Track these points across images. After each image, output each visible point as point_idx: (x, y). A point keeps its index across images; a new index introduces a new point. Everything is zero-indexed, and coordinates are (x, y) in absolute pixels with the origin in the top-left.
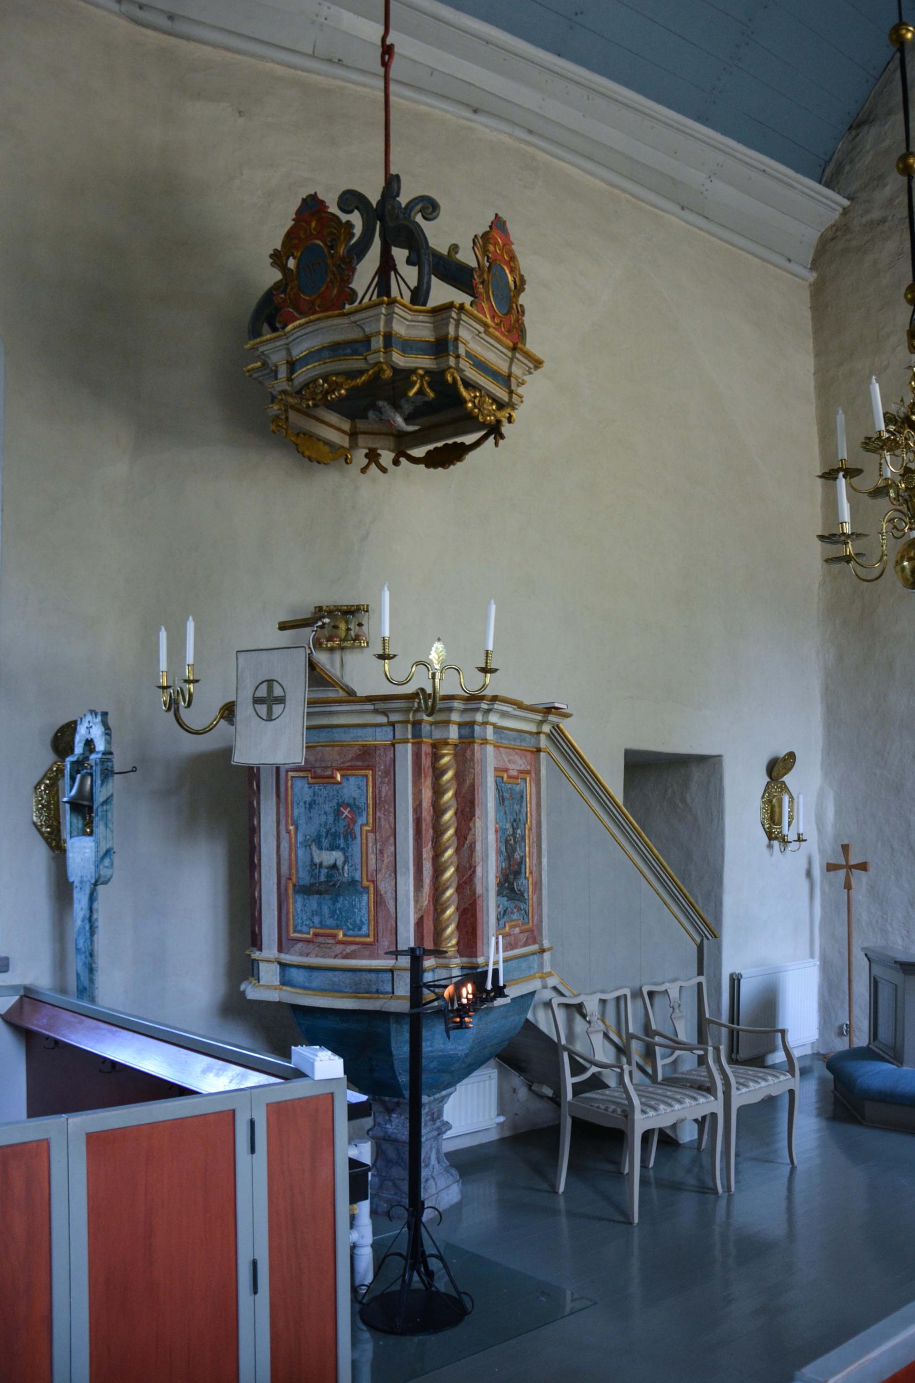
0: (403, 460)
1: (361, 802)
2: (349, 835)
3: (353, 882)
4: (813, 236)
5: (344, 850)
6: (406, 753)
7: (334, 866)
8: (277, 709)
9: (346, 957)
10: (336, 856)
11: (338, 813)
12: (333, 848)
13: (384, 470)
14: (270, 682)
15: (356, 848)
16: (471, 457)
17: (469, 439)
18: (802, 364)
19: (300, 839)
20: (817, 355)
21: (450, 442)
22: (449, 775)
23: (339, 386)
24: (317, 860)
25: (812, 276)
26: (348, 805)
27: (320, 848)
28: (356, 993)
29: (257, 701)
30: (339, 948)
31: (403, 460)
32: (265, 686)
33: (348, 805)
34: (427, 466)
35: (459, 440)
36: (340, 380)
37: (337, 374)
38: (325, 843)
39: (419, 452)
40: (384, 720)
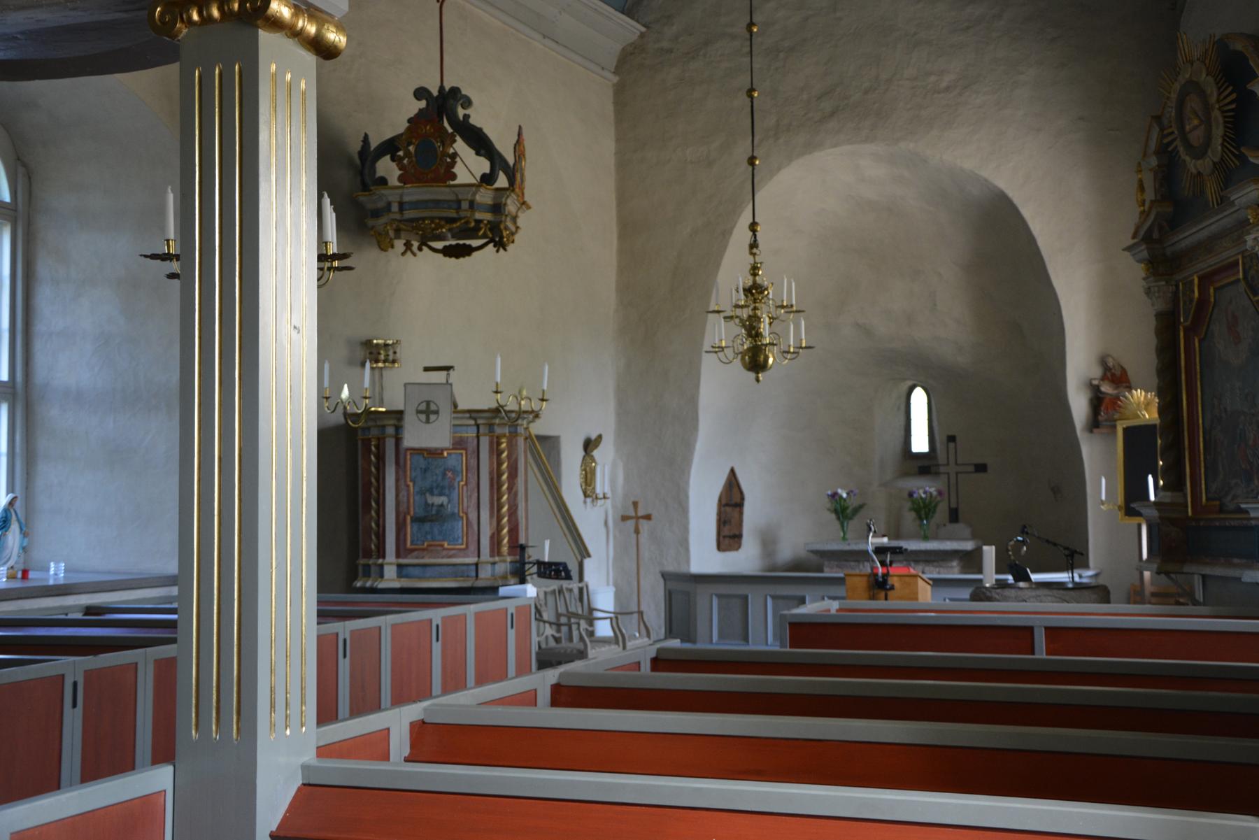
0: (425, 248)
1: (459, 468)
2: (451, 487)
3: (453, 514)
4: (618, 47)
5: (448, 496)
6: (485, 441)
7: (442, 505)
8: (433, 417)
9: (450, 557)
10: (443, 499)
11: (444, 475)
12: (441, 494)
13: (414, 255)
14: (428, 403)
15: (455, 495)
16: (475, 254)
17: (475, 243)
18: (607, 146)
19: (417, 489)
20: (618, 140)
21: (461, 242)
22: (505, 455)
23: (442, 227)
24: (430, 501)
25: (615, 79)
26: (450, 470)
27: (432, 494)
28: (455, 576)
29: (419, 412)
30: (444, 553)
31: (425, 248)
32: (424, 405)
33: (450, 470)
34: (445, 255)
35: (468, 242)
36: (443, 223)
37: (440, 218)
38: (436, 492)
39: (439, 245)
40: (472, 422)
